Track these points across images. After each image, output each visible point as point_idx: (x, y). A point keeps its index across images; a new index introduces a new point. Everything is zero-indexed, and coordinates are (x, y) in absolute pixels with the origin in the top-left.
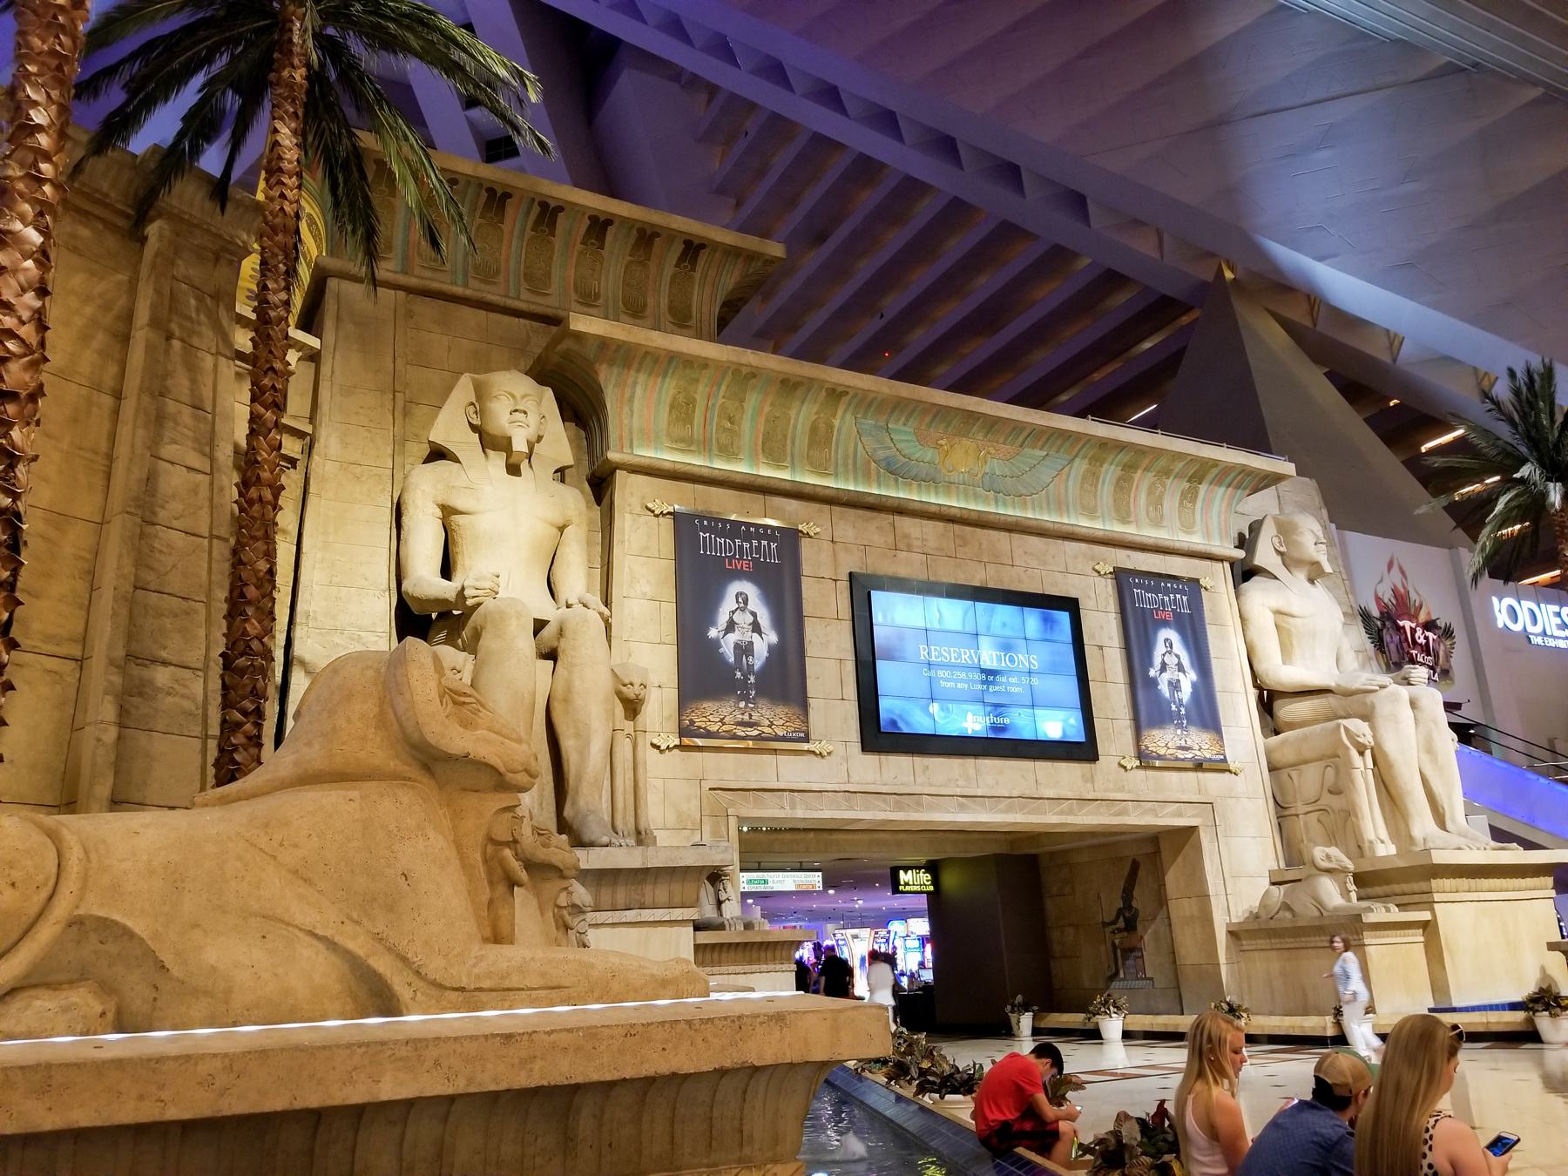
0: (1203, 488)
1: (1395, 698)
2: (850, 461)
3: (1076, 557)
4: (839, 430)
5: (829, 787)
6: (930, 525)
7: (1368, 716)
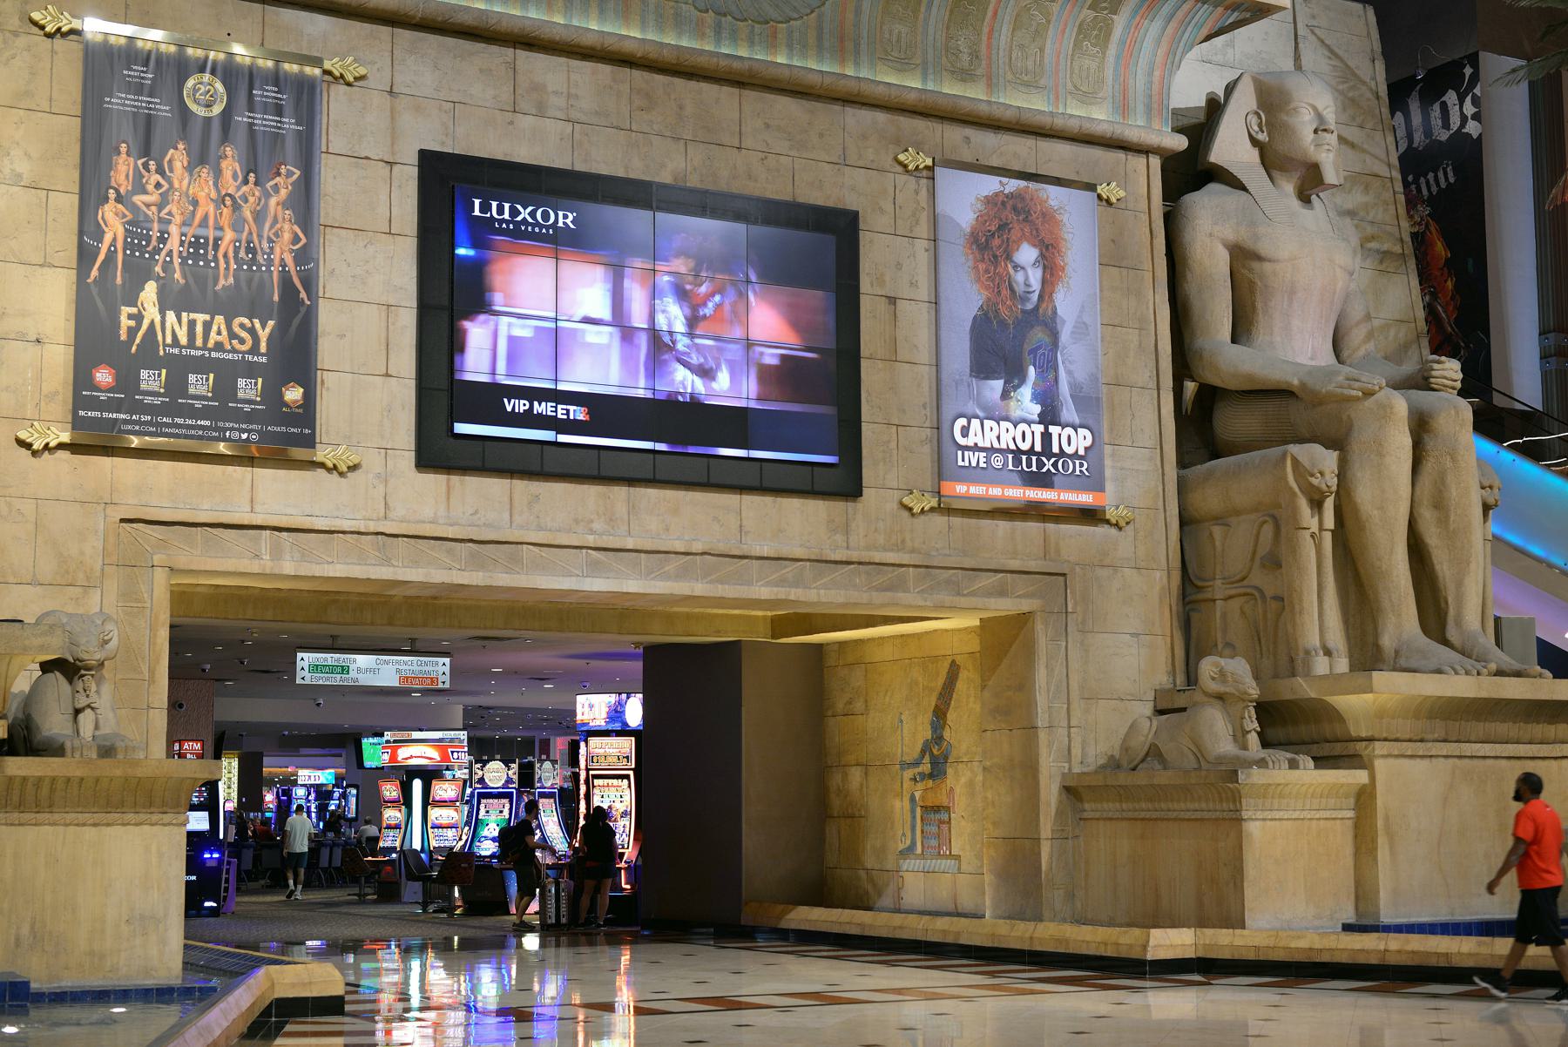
0: (1120, 22)
1: (1385, 412)
3: (864, 137)
5: (346, 525)
6: (584, 71)
7: (1337, 442)
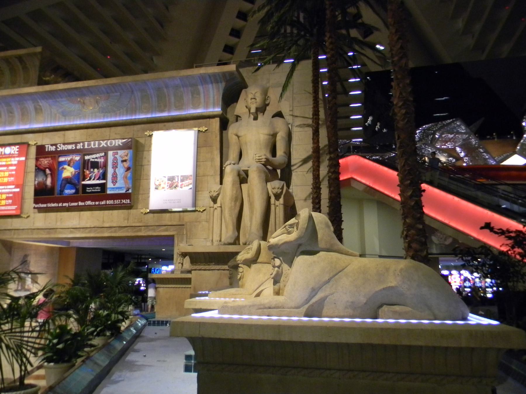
5: (26, 228)
6: (78, 131)
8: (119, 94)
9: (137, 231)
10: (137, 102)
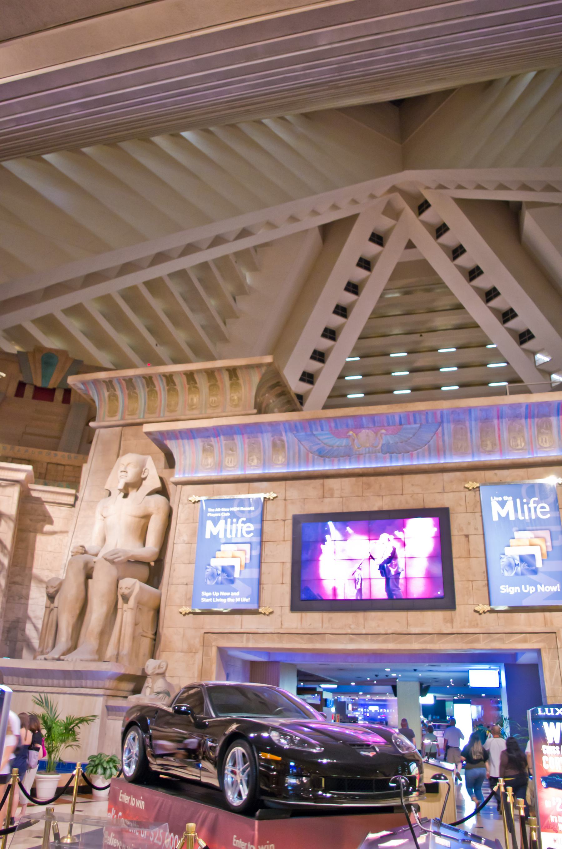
2: (297, 456)
4: (288, 441)
5: (268, 631)
6: (346, 481)
8: (418, 425)
9: (472, 642)
10: (446, 438)
